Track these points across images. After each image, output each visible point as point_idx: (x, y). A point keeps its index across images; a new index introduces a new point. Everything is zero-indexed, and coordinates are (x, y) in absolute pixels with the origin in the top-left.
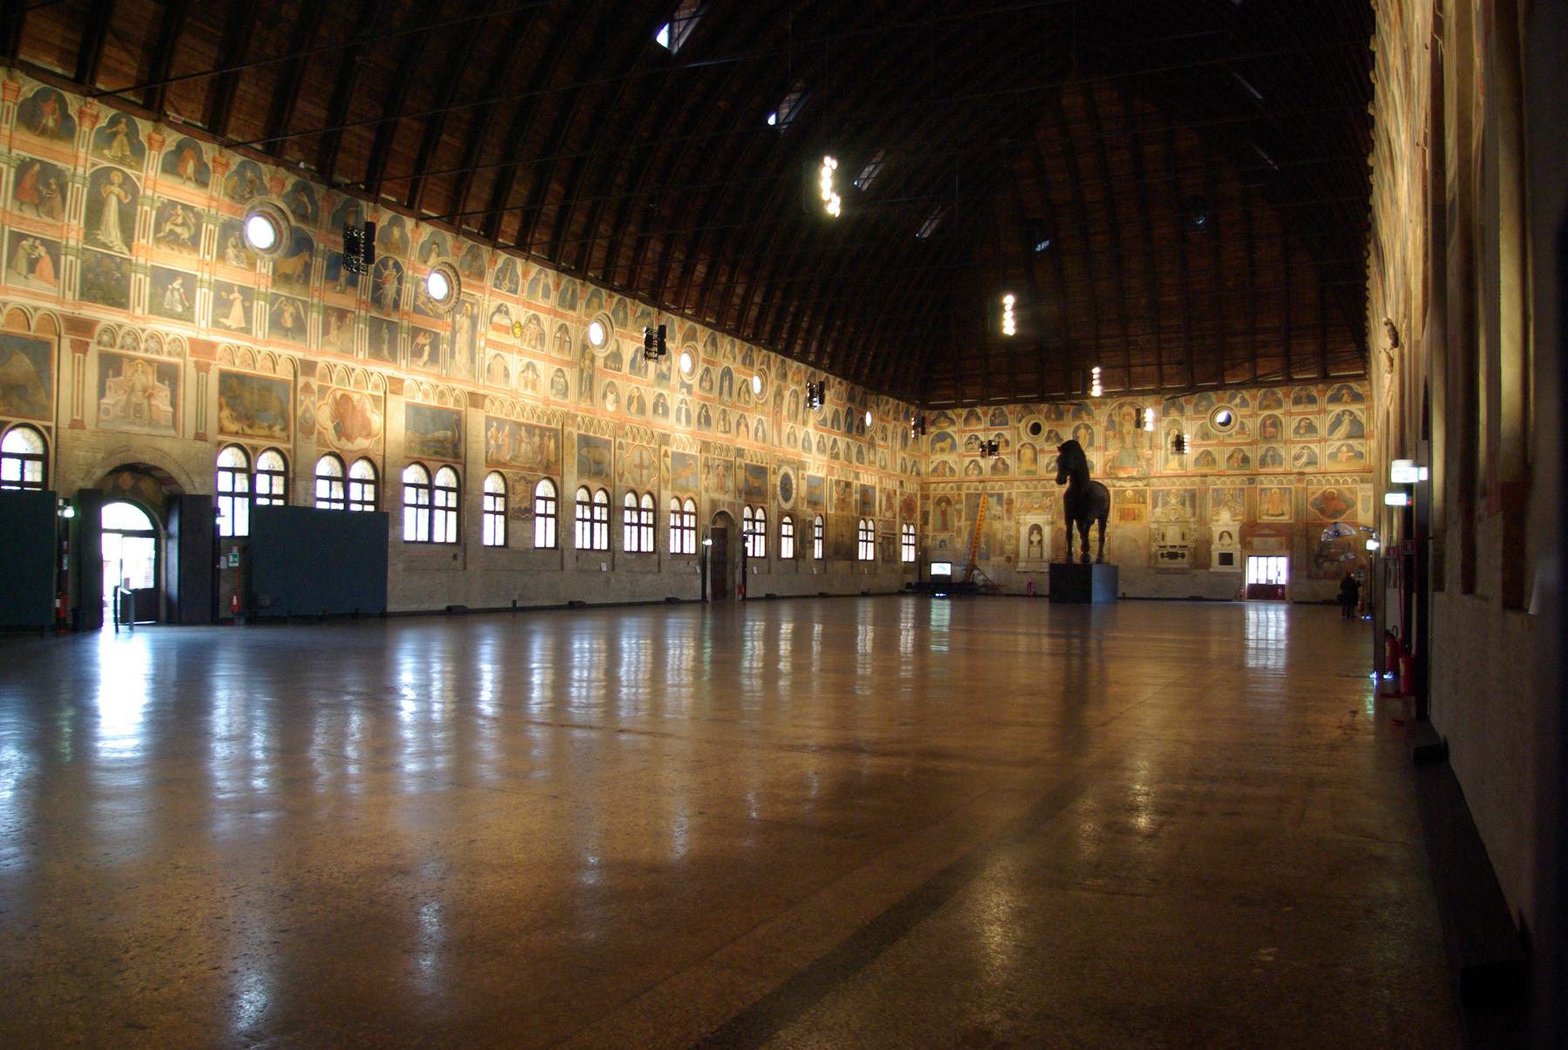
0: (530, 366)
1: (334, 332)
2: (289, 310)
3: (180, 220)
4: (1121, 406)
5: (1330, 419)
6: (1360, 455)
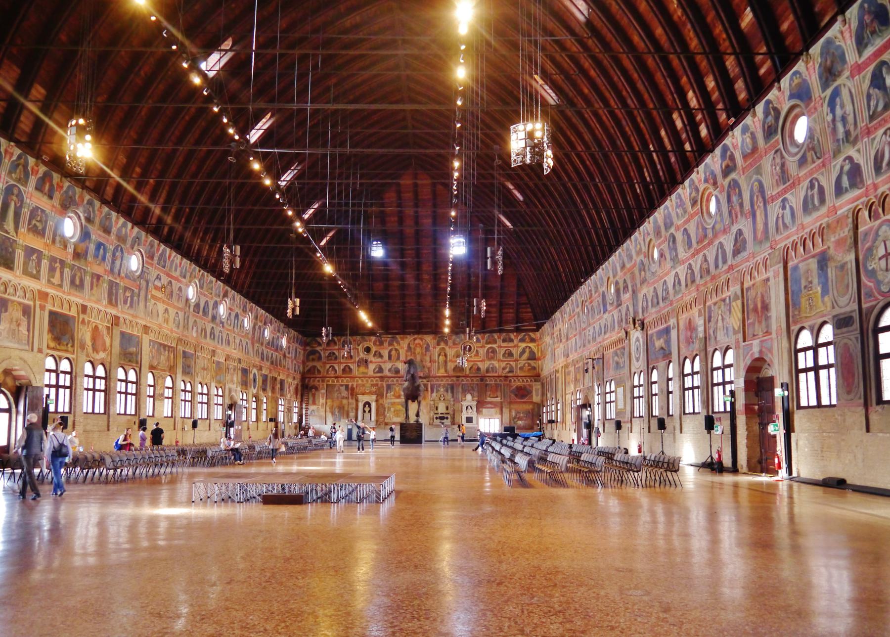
0: (166, 310)
1: (95, 288)
2: (79, 274)
3: (39, 219)
4: (415, 339)
5: (520, 349)
6: (534, 368)
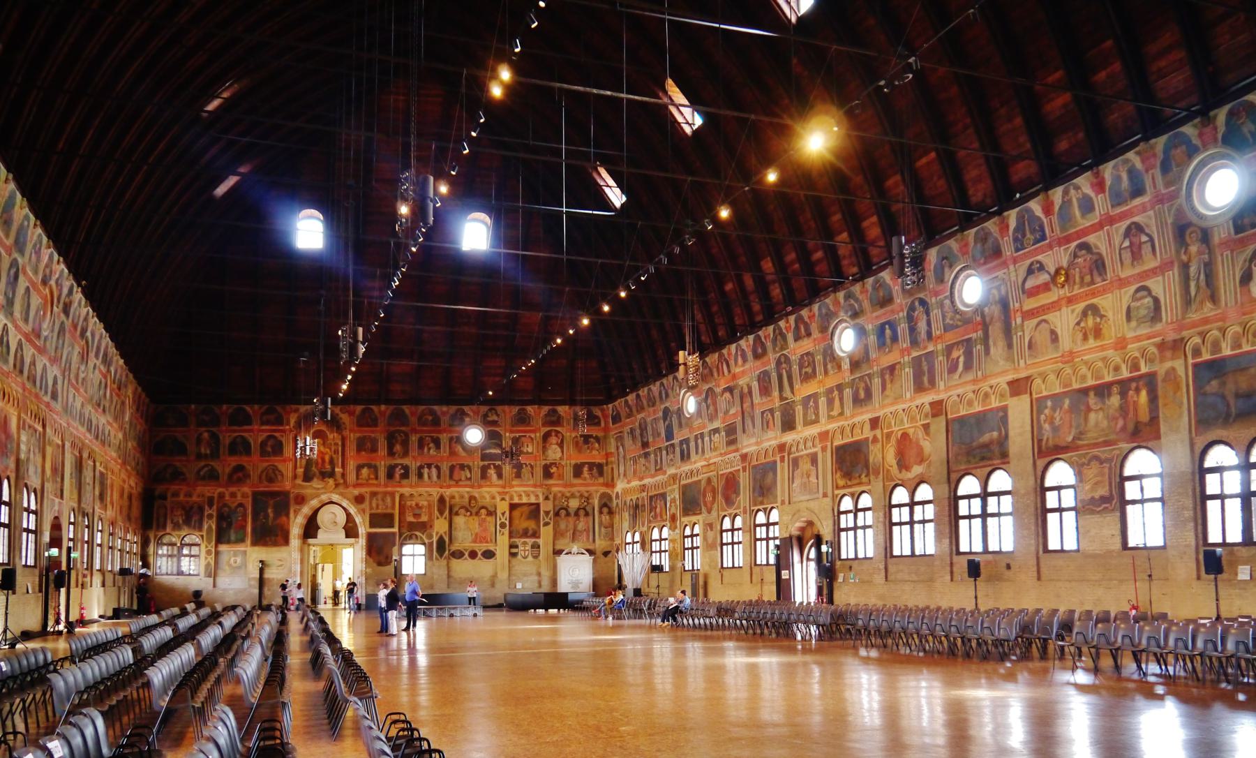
1: (889, 386)
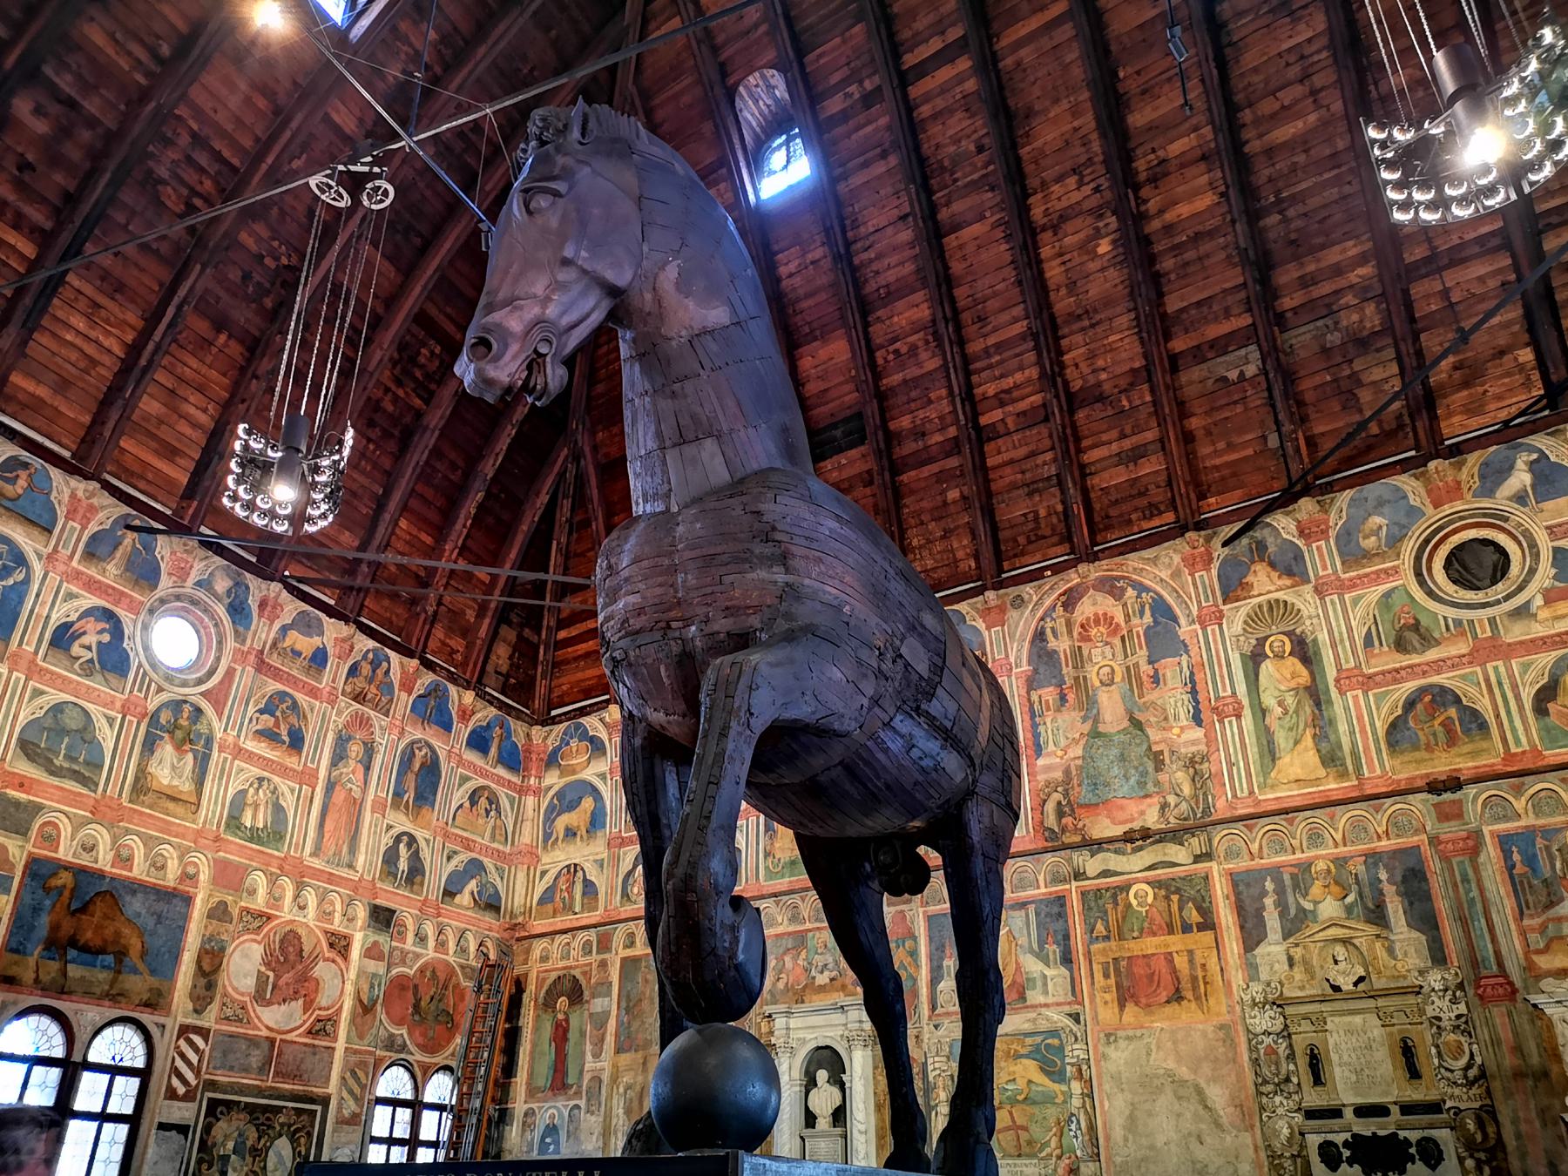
4: (1070, 600)
